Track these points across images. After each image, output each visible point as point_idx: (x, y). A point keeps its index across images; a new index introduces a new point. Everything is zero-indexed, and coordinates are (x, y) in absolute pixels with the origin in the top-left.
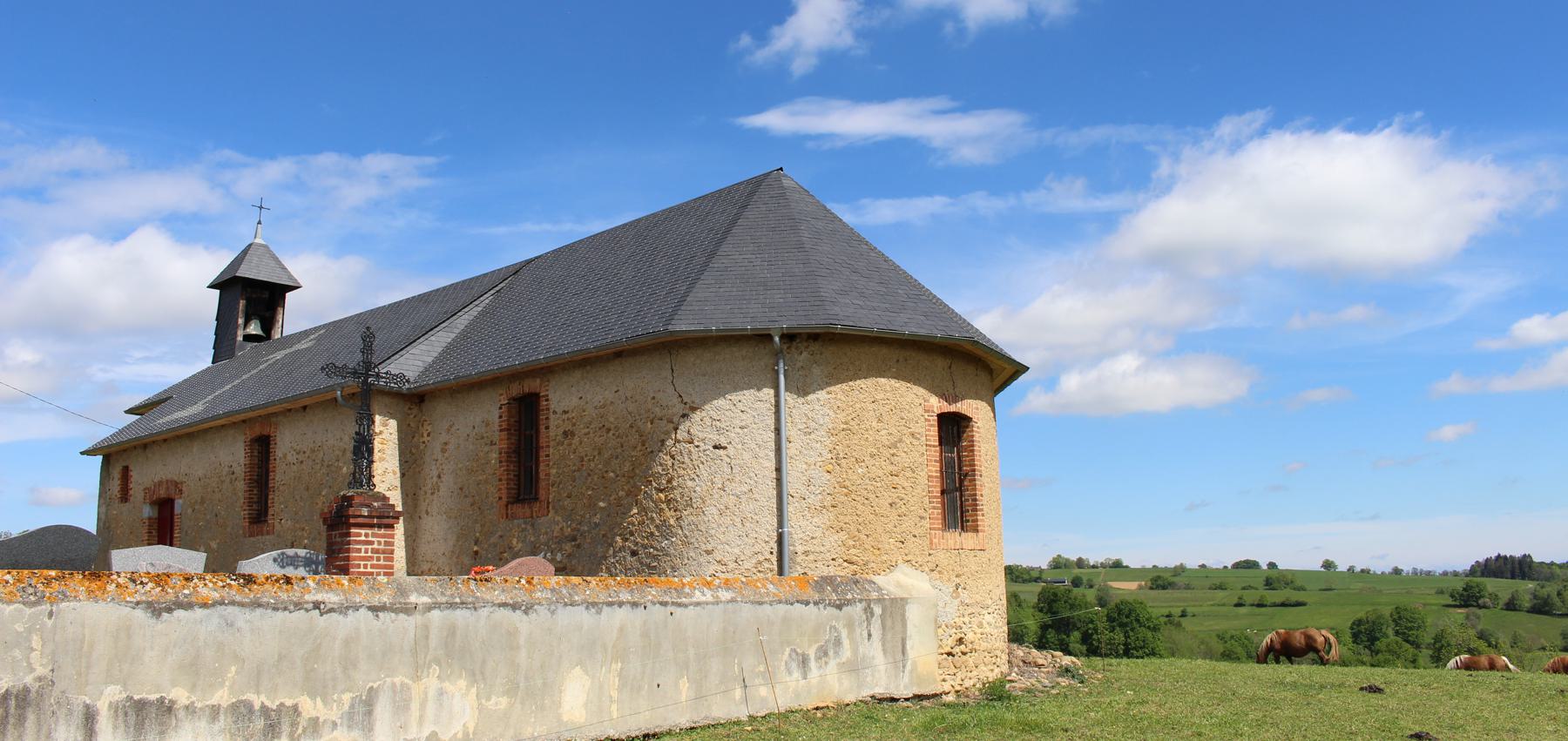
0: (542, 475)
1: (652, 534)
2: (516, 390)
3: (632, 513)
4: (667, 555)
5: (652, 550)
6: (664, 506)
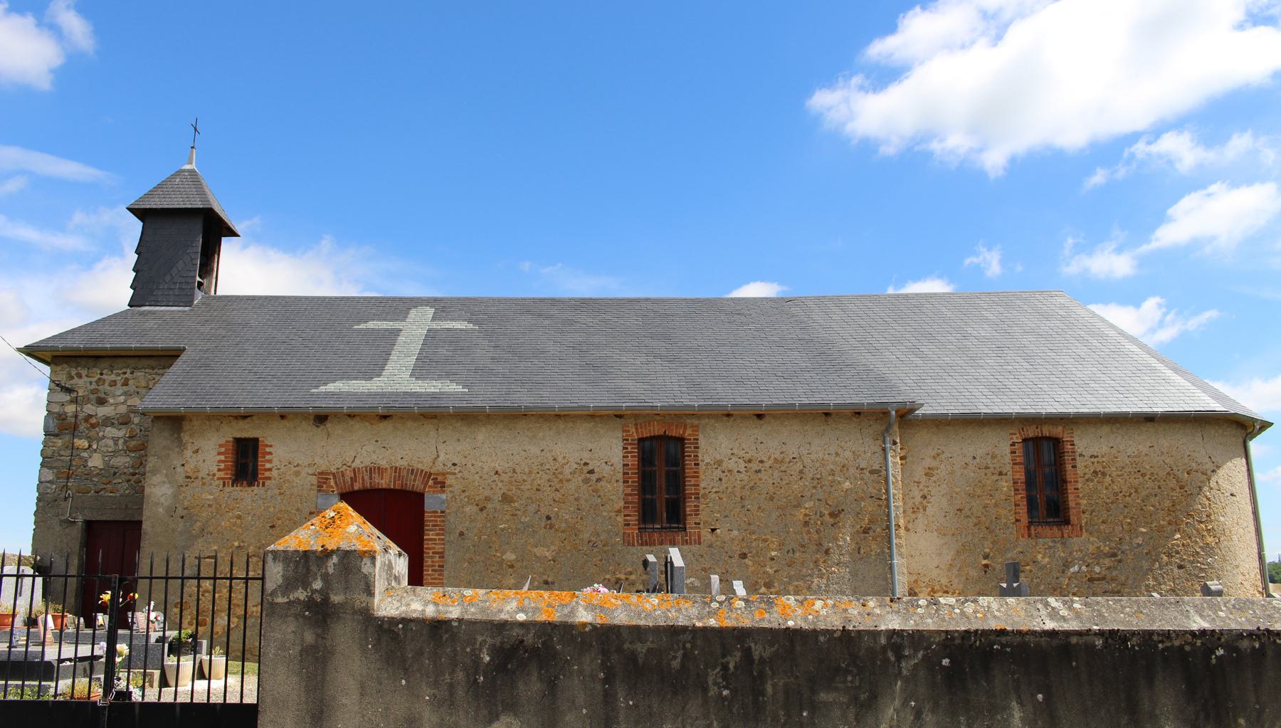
0: (1072, 504)
1: (1198, 553)
2: (1032, 432)
3: (1176, 537)
4: (1212, 568)
5: (1199, 565)
6: (1205, 533)
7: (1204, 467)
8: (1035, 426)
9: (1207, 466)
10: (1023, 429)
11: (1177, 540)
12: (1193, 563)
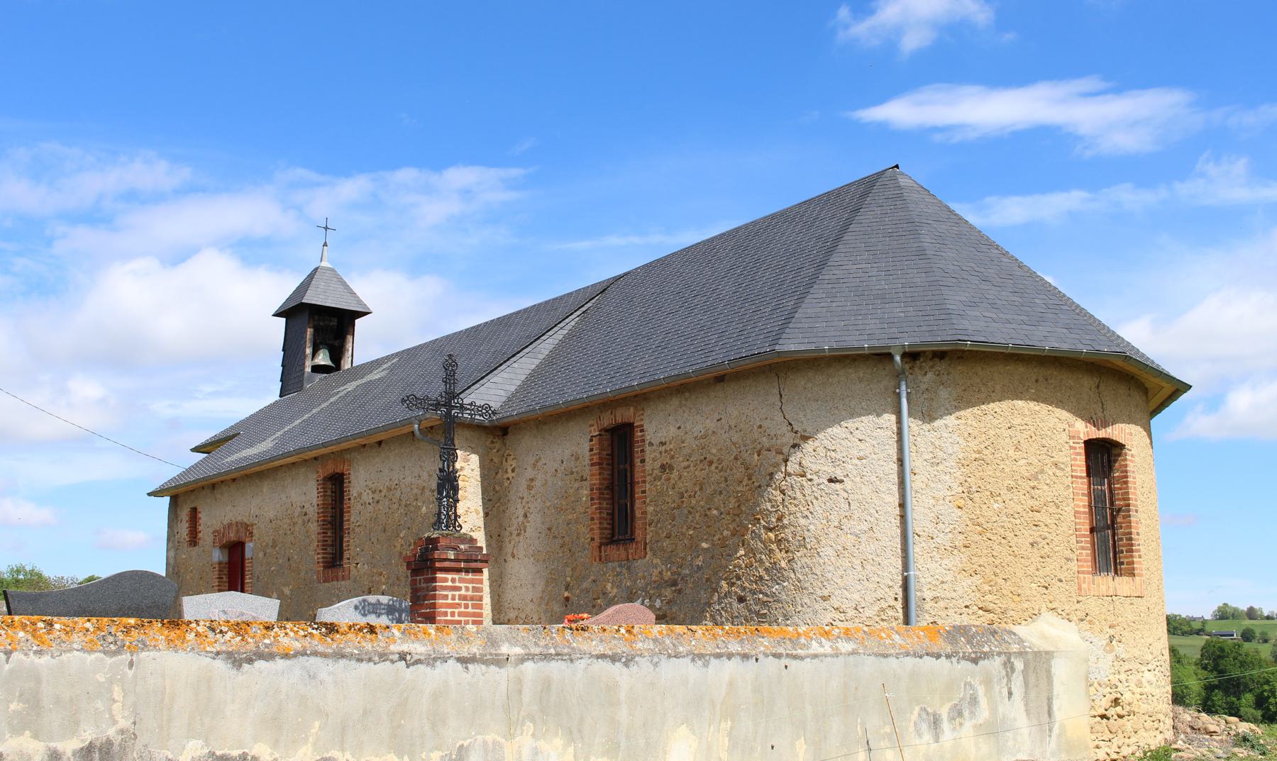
0: (638, 514)
1: (761, 578)
2: (607, 420)
3: (738, 555)
4: (778, 601)
5: (761, 596)
6: (774, 547)
7: (779, 441)
8: (609, 412)
9: (785, 440)
10: (600, 418)
11: (739, 558)
12: (754, 593)
